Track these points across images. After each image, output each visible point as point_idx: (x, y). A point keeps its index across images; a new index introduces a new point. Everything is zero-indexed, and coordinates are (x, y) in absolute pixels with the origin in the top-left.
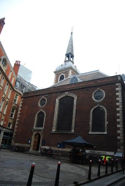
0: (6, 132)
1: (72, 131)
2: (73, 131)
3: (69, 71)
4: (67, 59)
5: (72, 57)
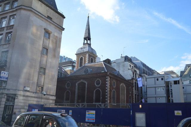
3: (86, 54)
4: (86, 42)
5: (90, 39)
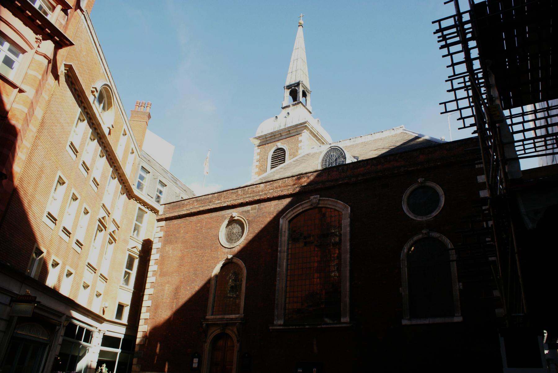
0: (108, 334)
1: (343, 320)
2: (345, 319)
